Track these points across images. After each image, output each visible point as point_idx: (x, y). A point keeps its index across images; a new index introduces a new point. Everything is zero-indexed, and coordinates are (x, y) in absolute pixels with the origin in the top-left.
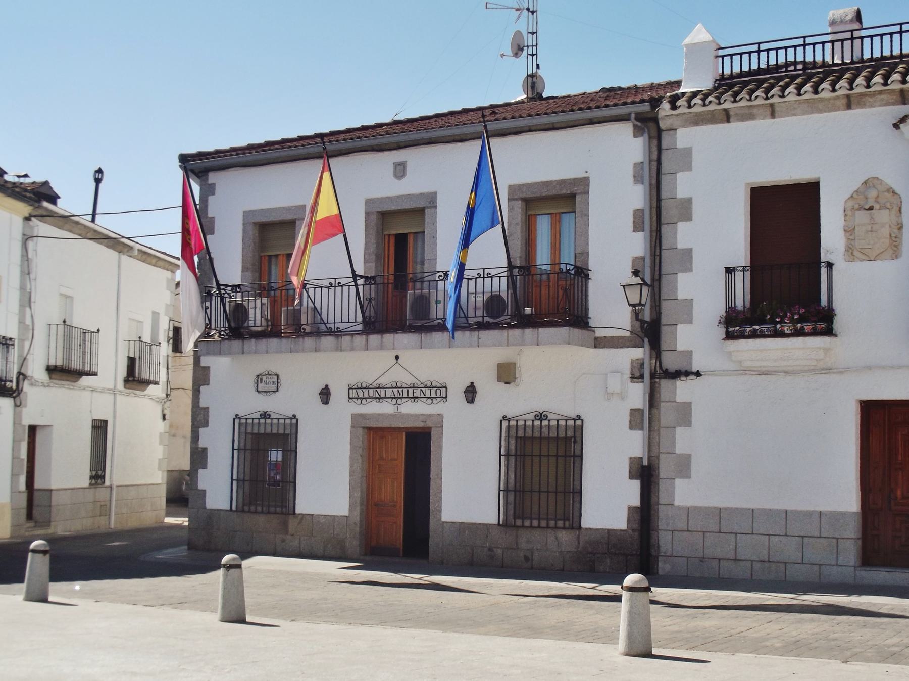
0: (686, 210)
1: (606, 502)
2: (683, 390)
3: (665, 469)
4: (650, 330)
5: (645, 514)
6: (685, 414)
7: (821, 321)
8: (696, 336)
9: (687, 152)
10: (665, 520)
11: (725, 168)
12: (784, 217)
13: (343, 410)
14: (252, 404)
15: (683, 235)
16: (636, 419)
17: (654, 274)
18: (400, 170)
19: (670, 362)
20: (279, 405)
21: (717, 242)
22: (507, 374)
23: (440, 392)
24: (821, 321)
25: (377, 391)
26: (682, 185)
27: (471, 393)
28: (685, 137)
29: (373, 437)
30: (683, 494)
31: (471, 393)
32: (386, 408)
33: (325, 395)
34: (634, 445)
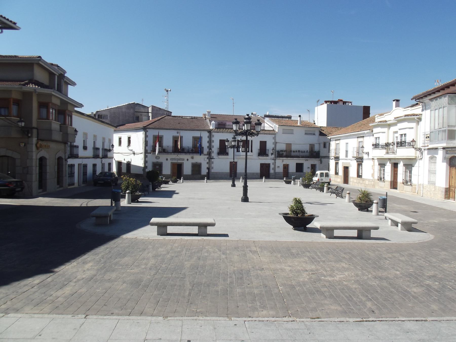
0: (213, 141)
1: (204, 171)
2: (213, 160)
3: (210, 168)
4: (209, 154)
5: (208, 173)
6: (213, 163)
7: (227, 154)
8: (214, 155)
9: (213, 135)
10: (210, 174)
11: (218, 137)
12: (222, 142)
13: (169, 162)
14: (155, 160)
15: (213, 144)
16: (208, 163)
17: (210, 147)
18: (178, 133)
19: (211, 157)
20: (159, 161)
21: (216, 145)
22: (192, 158)
23: (183, 160)
24: (227, 154)
25: (175, 159)
26: (213, 139)
27: (188, 160)
28: (213, 134)
29: (173, 165)
30: (213, 171)
31: (188, 160)
32: (176, 161)
33: (167, 159)
34: (207, 166)
